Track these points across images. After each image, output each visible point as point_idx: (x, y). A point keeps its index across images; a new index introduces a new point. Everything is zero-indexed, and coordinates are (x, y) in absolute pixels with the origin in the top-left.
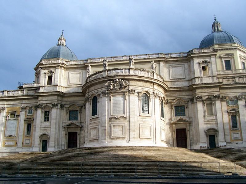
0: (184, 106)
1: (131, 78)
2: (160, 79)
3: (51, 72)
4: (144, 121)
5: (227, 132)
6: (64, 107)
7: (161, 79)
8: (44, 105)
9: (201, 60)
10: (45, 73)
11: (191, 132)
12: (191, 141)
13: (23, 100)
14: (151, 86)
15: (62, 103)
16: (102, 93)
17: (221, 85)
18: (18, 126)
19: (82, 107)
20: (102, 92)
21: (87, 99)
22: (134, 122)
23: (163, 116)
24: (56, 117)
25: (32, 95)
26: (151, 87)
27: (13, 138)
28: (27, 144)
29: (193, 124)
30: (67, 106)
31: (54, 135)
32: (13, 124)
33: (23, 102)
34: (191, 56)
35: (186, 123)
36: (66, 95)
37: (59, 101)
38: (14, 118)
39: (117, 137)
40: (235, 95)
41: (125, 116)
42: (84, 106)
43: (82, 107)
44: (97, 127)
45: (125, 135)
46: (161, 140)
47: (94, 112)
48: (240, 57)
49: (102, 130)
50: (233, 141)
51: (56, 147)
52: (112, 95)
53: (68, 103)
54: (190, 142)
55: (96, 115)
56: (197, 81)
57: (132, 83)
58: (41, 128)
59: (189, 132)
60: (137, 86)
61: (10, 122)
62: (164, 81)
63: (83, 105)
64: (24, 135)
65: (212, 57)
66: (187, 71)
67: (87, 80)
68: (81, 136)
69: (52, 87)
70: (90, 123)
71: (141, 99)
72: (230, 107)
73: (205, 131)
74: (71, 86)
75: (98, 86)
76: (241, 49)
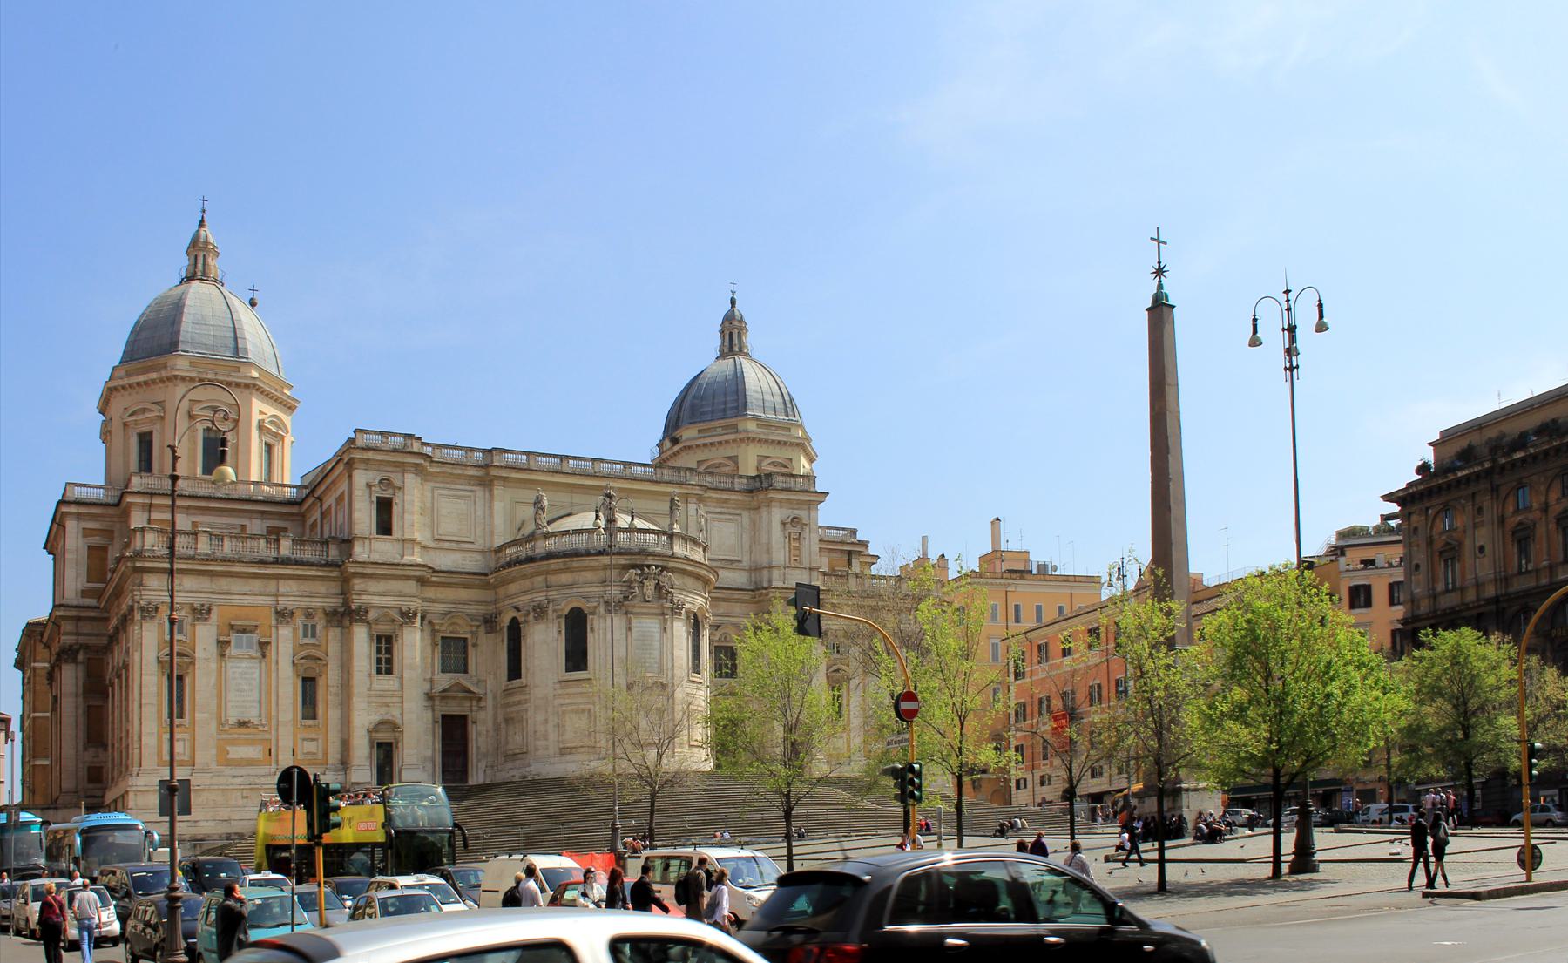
3: (385, 482)
27: (255, 730)
28: (309, 757)
32: (247, 676)
61: (239, 667)
64: (295, 719)
69: (395, 543)
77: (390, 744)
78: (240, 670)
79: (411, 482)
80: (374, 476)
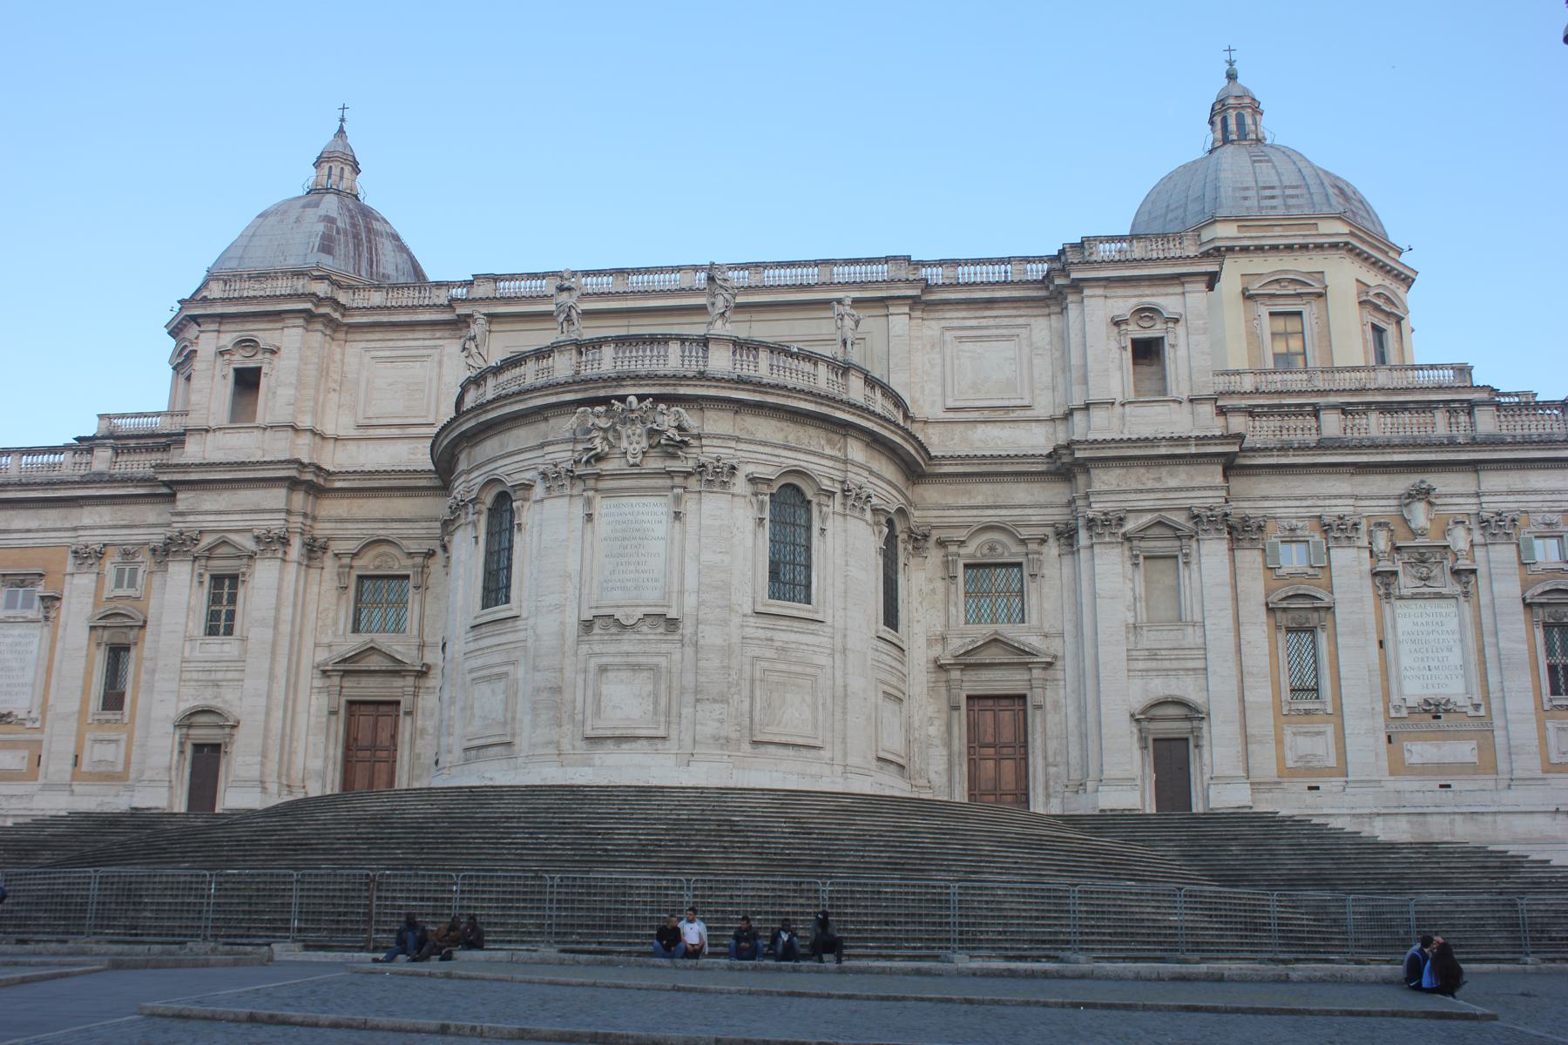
0: (1019, 565)
1: (712, 392)
2: (880, 404)
3: (248, 343)
4: (777, 644)
5: (1262, 723)
6: (330, 553)
7: (891, 407)
8: (207, 540)
9: (1124, 303)
10: (222, 353)
11: (1052, 718)
12: (1052, 770)
13: (87, 510)
14: (829, 441)
15: (317, 533)
16: (544, 475)
17: (1236, 449)
18: (51, 660)
19: (430, 554)
20: (541, 468)
21: (460, 506)
22: (727, 651)
23: (891, 617)
24: (278, 609)
25: (143, 481)
26: (828, 451)
27: (20, 728)
28: (102, 769)
29: (1069, 665)
30: (352, 546)
31: (262, 717)
33: (87, 521)
34: (1073, 275)
35: (1026, 666)
36: (338, 485)
37: (301, 519)
38: (32, 614)
39: (618, 733)
40: (1316, 512)
41: (672, 614)
42: (439, 551)
43: (430, 554)
44: (506, 674)
45: (668, 723)
46: (880, 759)
47: (496, 586)
48: (1359, 295)
49: (538, 690)
50: (1293, 773)
51: (273, 787)
52: (596, 490)
53: (352, 529)
54: (1046, 774)
55: (507, 601)
56: (1101, 426)
57: (717, 423)
58: (186, 676)
59: (1038, 720)
60: (750, 442)
62: (906, 416)
63: (435, 545)
64: (83, 712)
65: (1188, 287)
66: (1043, 368)
67: (460, 400)
68: (419, 723)
69: (256, 433)
70: (472, 646)
71: (767, 515)
72: (1280, 578)
73: (1132, 716)
74: (372, 432)
75: (522, 436)
76: (1365, 248)
77: (216, 748)
78: (10, 640)
79: (291, 339)
80: (227, 340)
